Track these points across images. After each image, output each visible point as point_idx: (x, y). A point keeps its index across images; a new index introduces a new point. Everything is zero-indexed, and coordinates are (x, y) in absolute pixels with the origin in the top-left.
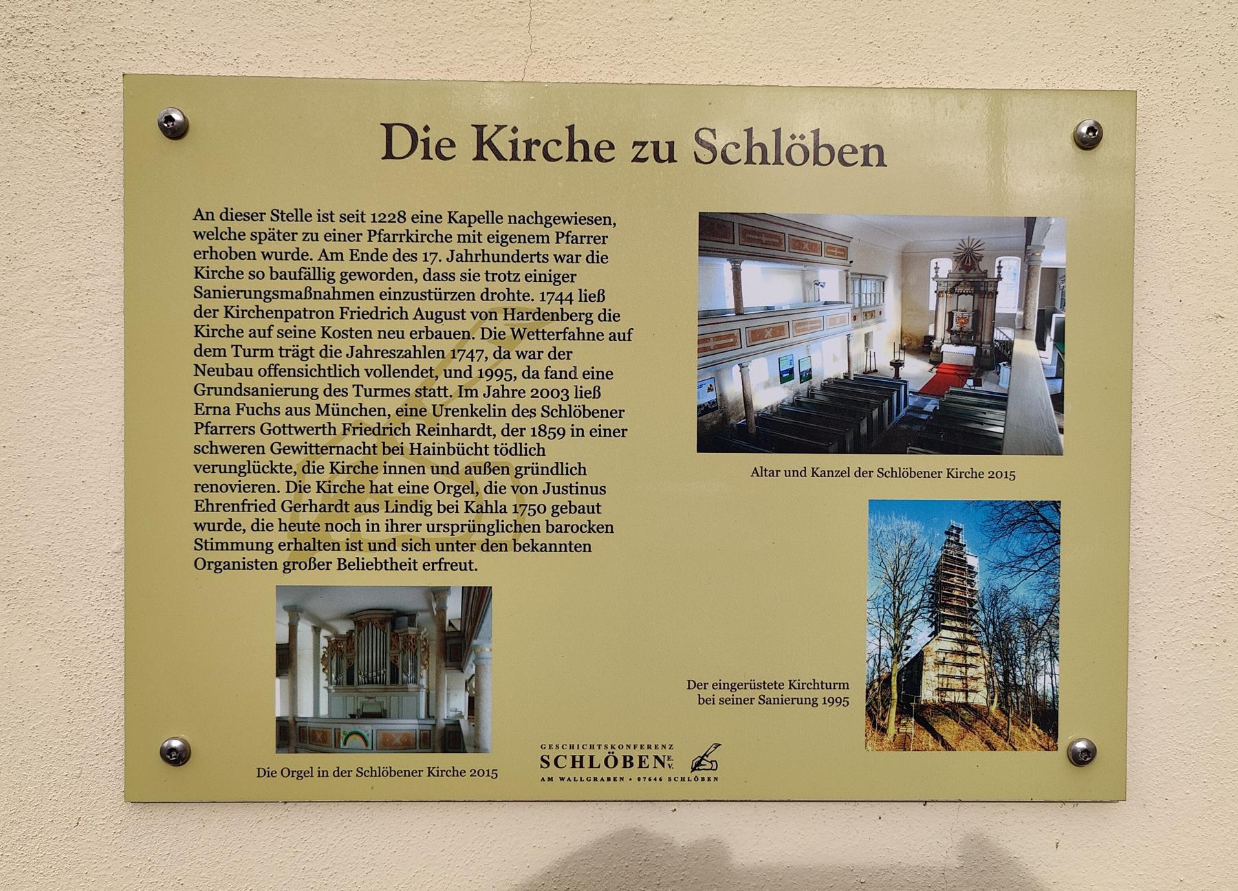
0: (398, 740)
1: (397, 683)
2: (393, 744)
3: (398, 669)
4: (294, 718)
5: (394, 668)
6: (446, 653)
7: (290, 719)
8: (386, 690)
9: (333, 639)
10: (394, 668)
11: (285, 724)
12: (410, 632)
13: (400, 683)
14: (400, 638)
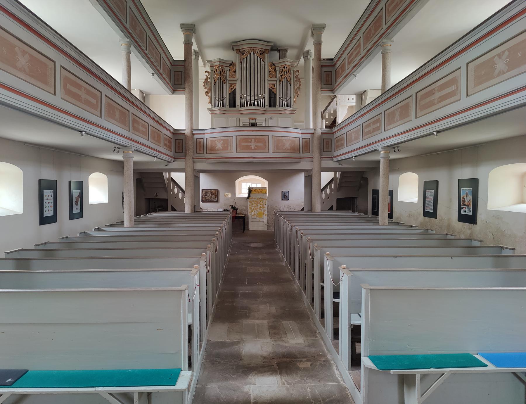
0: (287, 145)
1: (275, 106)
2: (284, 148)
3: (275, 94)
4: (192, 130)
5: (272, 93)
6: (321, 79)
7: (187, 132)
8: (265, 113)
9: (218, 63)
10: (272, 93)
11: (182, 137)
12: (287, 63)
13: (277, 106)
14: (277, 68)
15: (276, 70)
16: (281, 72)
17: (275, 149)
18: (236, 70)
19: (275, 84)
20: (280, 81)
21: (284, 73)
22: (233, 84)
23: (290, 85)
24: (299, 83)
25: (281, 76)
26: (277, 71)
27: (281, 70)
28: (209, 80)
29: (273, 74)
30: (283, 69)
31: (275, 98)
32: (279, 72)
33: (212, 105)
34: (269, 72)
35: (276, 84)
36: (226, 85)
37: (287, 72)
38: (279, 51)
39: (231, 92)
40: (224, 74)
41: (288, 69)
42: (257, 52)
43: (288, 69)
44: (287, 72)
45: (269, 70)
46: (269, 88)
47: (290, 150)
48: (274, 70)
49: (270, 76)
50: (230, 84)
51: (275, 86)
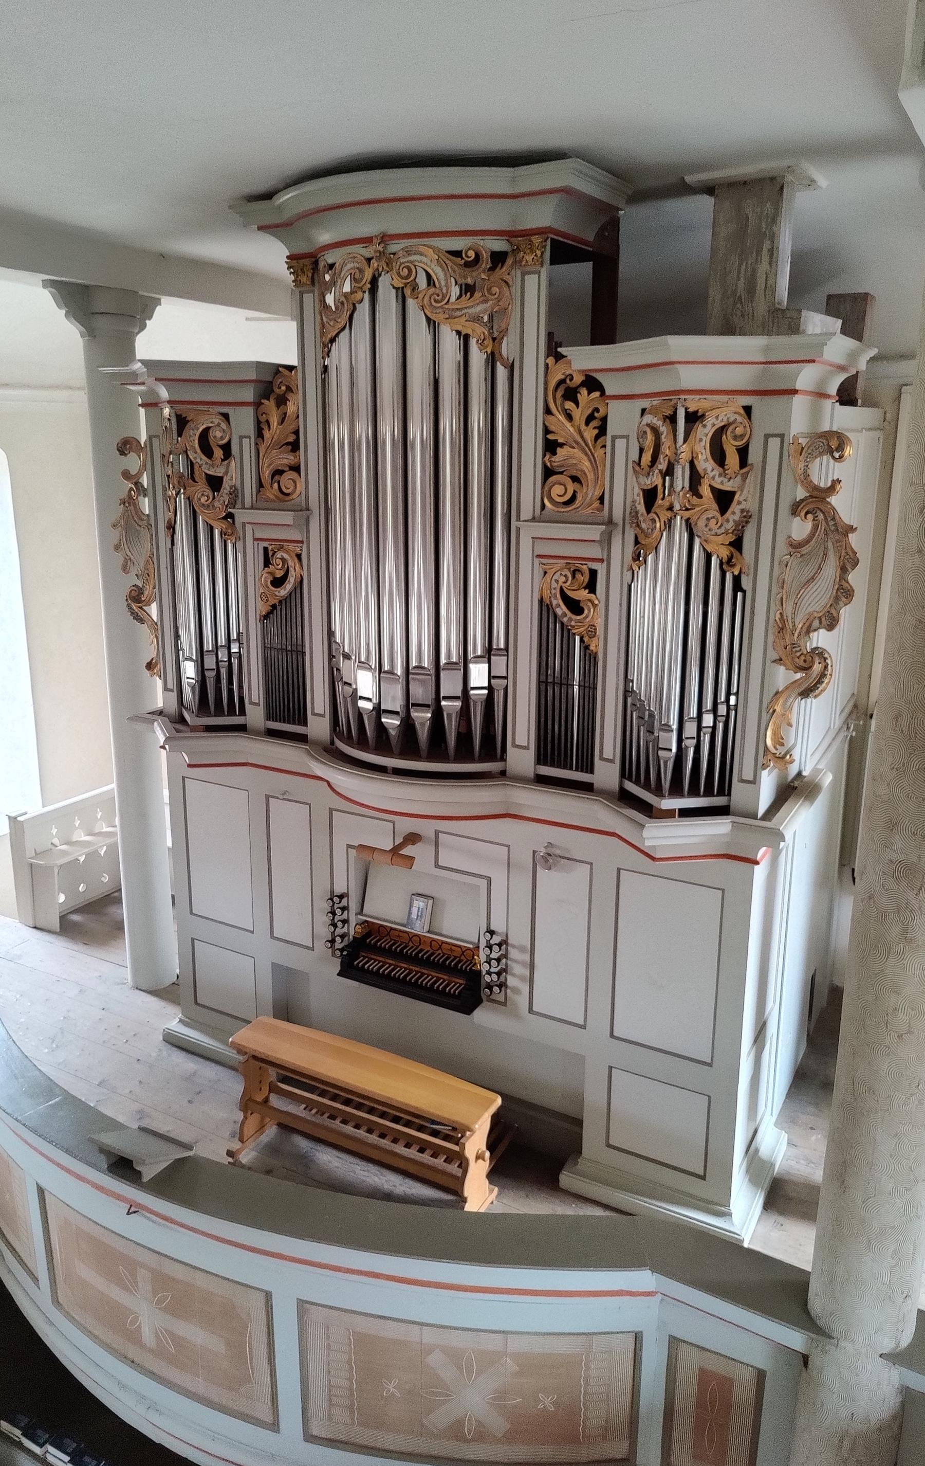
2: (441, 1418)
3: (590, 658)
12: (689, 377)
15: (611, 430)
16: (647, 458)
17: (340, 1415)
18: (297, 433)
19: (594, 566)
20: (637, 542)
21: (669, 471)
22: (281, 544)
23: (737, 586)
24: (830, 570)
25: (650, 496)
26: (620, 444)
27: (650, 437)
28: (145, 505)
29: (586, 465)
30: (664, 429)
31: (590, 688)
32: (634, 455)
33: (170, 686)
34: (551, 447)
35: (601, 568)
36: (239, 545)
37: (706, 464)
38: (710, 190)
39: (274, 607)
40: (218, 472)
41: (704, 433)
42: (429, 276)
43: (704, 433)
44: (706, 464)
45: (547, 431)
46: (541, 601)
47: (510, 1437)
48: (590, 433)
49: (557, 490)
50: (266, 544)
51: (591, 587)
